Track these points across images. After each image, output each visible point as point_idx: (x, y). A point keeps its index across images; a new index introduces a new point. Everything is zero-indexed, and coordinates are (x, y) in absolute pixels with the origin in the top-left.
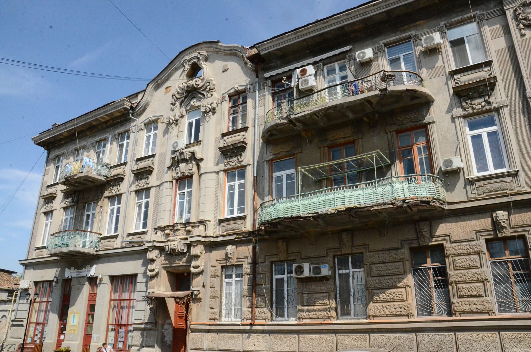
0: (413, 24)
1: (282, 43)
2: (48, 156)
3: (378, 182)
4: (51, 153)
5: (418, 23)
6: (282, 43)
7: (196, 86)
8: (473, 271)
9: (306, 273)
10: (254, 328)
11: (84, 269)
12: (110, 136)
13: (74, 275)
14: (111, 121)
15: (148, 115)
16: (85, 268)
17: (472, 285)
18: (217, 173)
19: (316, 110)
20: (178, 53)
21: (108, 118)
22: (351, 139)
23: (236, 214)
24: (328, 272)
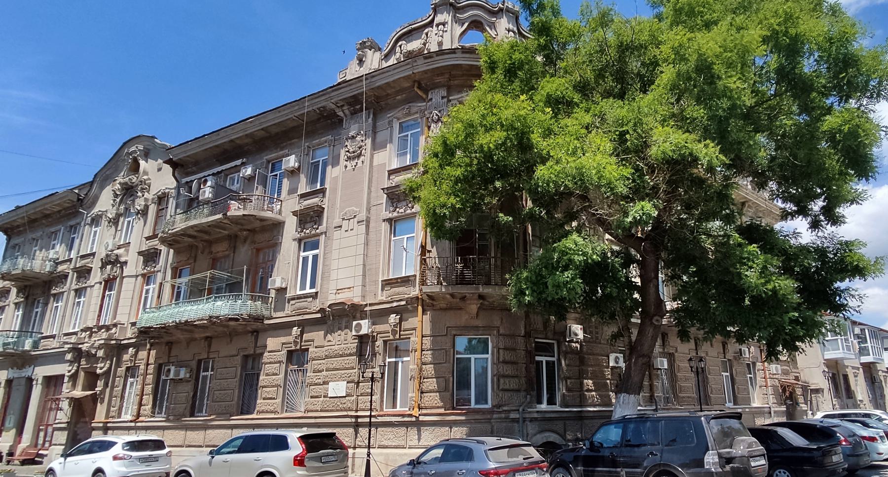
0: (289, 142)
1: (216, 140)
2: (8, 244)
3: (207, 299)
4: (11, 240)
5: (293, 141)
6: (216, 140)
7: (130, 184)
8: (274, 377)
9: (171, 376)
10: (139, 424)
11: (24, 370)
12: (62, 228)
13: (16, 376)
14: (63, 211)
15: (96, 210)
16: (25, 368)
17: (271, 389)
18: (137, 276)
19: (183, 227)
20: (121, 144)
21: (58, 208)
22: (227, 253)
23: (308, 290)
24: (185, 374)
